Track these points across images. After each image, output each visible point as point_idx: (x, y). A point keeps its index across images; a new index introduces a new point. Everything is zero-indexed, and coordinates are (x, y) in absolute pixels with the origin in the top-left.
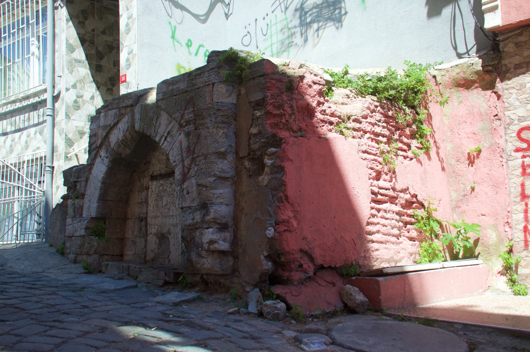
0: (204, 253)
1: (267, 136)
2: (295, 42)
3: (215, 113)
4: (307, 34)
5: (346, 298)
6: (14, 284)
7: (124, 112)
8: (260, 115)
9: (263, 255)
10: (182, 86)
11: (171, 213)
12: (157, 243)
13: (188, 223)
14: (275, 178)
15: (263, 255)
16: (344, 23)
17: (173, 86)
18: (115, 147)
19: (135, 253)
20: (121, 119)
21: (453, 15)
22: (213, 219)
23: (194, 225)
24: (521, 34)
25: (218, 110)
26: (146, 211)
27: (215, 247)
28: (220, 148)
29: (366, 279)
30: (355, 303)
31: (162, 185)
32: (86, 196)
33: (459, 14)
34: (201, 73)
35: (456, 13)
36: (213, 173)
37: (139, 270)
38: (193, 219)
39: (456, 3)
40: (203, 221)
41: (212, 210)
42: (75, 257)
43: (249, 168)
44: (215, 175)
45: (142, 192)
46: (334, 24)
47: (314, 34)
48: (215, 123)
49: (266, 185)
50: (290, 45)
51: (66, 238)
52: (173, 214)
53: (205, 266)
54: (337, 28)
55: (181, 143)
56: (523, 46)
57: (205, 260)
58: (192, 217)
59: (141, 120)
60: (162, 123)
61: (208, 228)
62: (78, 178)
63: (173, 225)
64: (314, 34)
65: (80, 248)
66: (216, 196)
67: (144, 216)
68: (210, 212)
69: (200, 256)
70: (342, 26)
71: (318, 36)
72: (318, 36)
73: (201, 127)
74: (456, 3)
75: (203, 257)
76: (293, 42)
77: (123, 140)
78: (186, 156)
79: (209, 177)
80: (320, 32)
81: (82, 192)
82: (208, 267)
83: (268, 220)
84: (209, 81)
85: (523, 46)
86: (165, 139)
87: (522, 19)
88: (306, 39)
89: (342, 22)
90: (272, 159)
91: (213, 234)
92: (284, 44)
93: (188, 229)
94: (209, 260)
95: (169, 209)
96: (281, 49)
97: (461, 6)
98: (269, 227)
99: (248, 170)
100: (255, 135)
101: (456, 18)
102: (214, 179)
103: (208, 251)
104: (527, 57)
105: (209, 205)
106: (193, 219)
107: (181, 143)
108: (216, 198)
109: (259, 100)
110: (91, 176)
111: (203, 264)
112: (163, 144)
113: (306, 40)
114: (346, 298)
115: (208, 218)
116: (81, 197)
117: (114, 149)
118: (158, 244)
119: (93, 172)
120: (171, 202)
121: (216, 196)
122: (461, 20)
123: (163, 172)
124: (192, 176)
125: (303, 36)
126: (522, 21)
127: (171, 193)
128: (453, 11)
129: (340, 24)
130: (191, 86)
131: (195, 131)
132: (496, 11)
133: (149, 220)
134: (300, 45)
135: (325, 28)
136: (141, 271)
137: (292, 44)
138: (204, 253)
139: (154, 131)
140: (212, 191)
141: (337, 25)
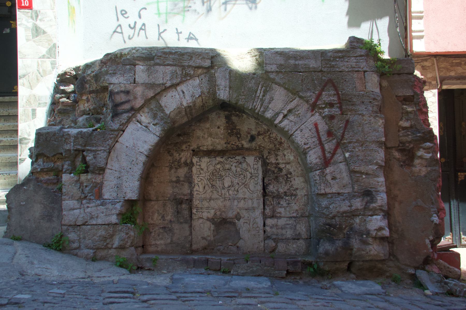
0: (370, 240)
1: (423, 131)
2: (193, 8)
3: (370, 102)
4: (210, 4)
5: (445, 271)
6: (323, 297)
7: (192, 73)
8: (412, 111)
9: (429, 239)
10: (313, 64)
11: (241, 195)
12: (212, 229)
13: (341, 210)
14: (435, 170)
15: (429, 239)
16: (259, 6)
17: (296, 61)
18: (172, 114)
19: (172, 241)
20: (185, 81)
21: (371, 30)
22: (379, 206)
23: (351, 212)
24: (426, 60)
25: (374, 99)
26: (189, 191)
27: (383, 234)
28: (381, 138)
29: (447, 254)
30: (456, 274)
31: (219, 163)
32: (107, 171)
33: (376, 30)
34: (343, 57)
35: (374, 29)
36: (375, 161)
37: (233, 262)
38: (351, 206)
39: (374, 21)
40: (366, 208)
41: (379, 198)
42: (94, 253)
43: (399, 158)
44: (377, 164)
45: (176, 169)
46: (247, 4)
47: (220, 6)
48: (372, 111)
49: (425, 176)
50: (186, 9)
51: (64, 228)
52: (246, 196)
53: (372, 253)
54: (251, 9)
55: (316, 125)
56: (427, 69)
57: (371, 247)
58: (349, 204)
59: (230, 88)
60: (276, 97)
61: (372, 216)
62: (85, 146)
63: (246, 209)
64: (220, 6)
65: (105, 241)
66: (380, 184)
67: (188, 197)
68: (377, 200)
69: (365, 243)
70: (256, 8)
71: (225, 10)
72: (225, 10)
73: (349, 113)
74: (374, 21)
75: (369, 244)
76: (190, 7)
77: (189, 107)
78: (326, 140)
79: (371, 165)
80: (229, 7)
81: (102, 165)
82: (375, 253)
83: (432, 208)
84: (360, 67)
85: (427, 69)
86: (285, 116)
87: (438, 51)
88: (209, 8)
89: (257, 4)
90: (429, 153)
91: (381, 221)
92: (178, 6)
93: (343, 216)
94: (375, 247)
95: (238, 191)
96: (172, 10)
97: (378, 25)
98: (434, 214)
99: (398, 160)
100: (404, 128)
101: (374, 33)
102: (376, 167)
103: (375, 238)
104: (430, 78)
105: (374, 193)
106: (351, 206)
107: (316, 125)
108: (380, 186)
109: (408, 96)
110: (118, 145)
111: (370, 251)
112: (281, 122)
113: (209, 10)
114: (445, 271)
115: (374, 205)
116: (97, 172)
117: (171, 115)
118: (214, 230)
119: (120, 140)
120: (240, 184)
121: (380, 184)
122: (378, 36)
123: (219, 148)
124: (339, 161)
125: (205, 4)
126: (437, 52)
127: (241, 173)
128: (371, 26)
129: (254, 6)
130: (328, 67)
131: (341, 116)
132: (422, 40)
133: (196, 202)
134: (201, 13)
135: (234, 4)
136: (234, 263)
137: (189, 9)
138: (370, 240)
139: (262, 105)
140: (375, 179)
141: (250, 5)
